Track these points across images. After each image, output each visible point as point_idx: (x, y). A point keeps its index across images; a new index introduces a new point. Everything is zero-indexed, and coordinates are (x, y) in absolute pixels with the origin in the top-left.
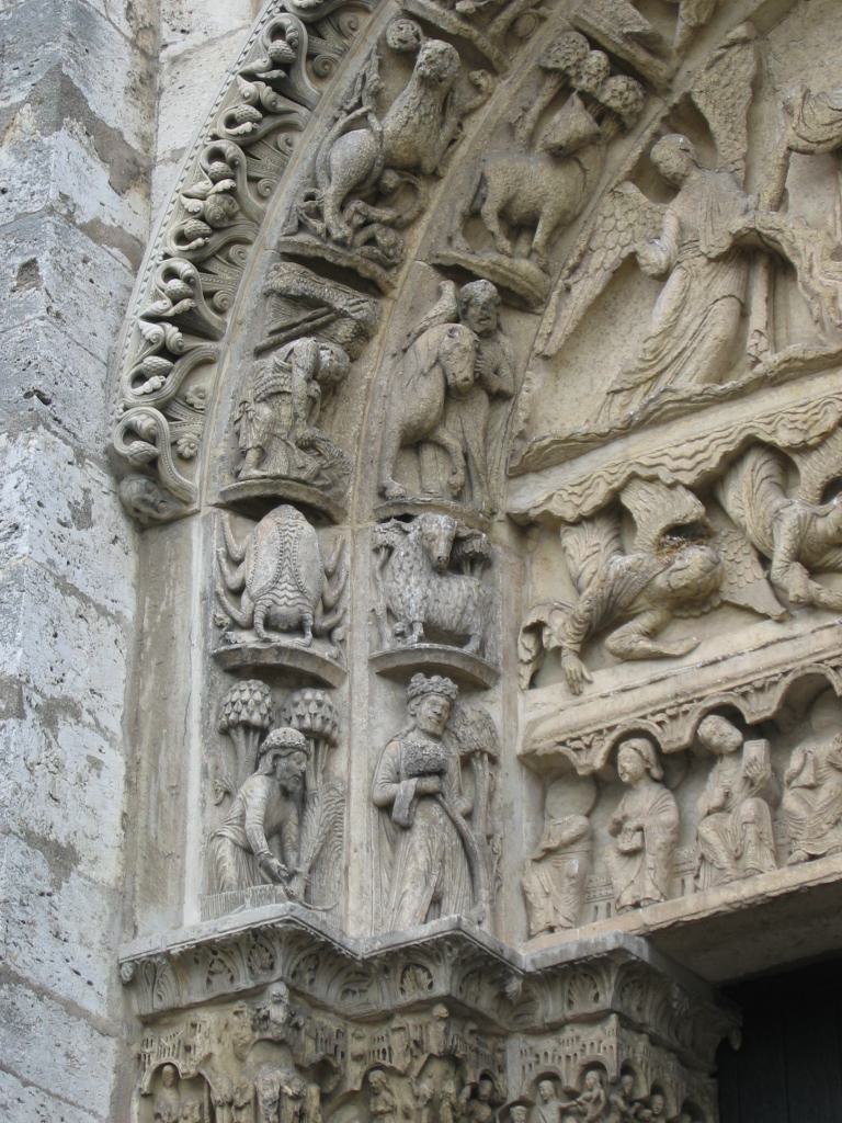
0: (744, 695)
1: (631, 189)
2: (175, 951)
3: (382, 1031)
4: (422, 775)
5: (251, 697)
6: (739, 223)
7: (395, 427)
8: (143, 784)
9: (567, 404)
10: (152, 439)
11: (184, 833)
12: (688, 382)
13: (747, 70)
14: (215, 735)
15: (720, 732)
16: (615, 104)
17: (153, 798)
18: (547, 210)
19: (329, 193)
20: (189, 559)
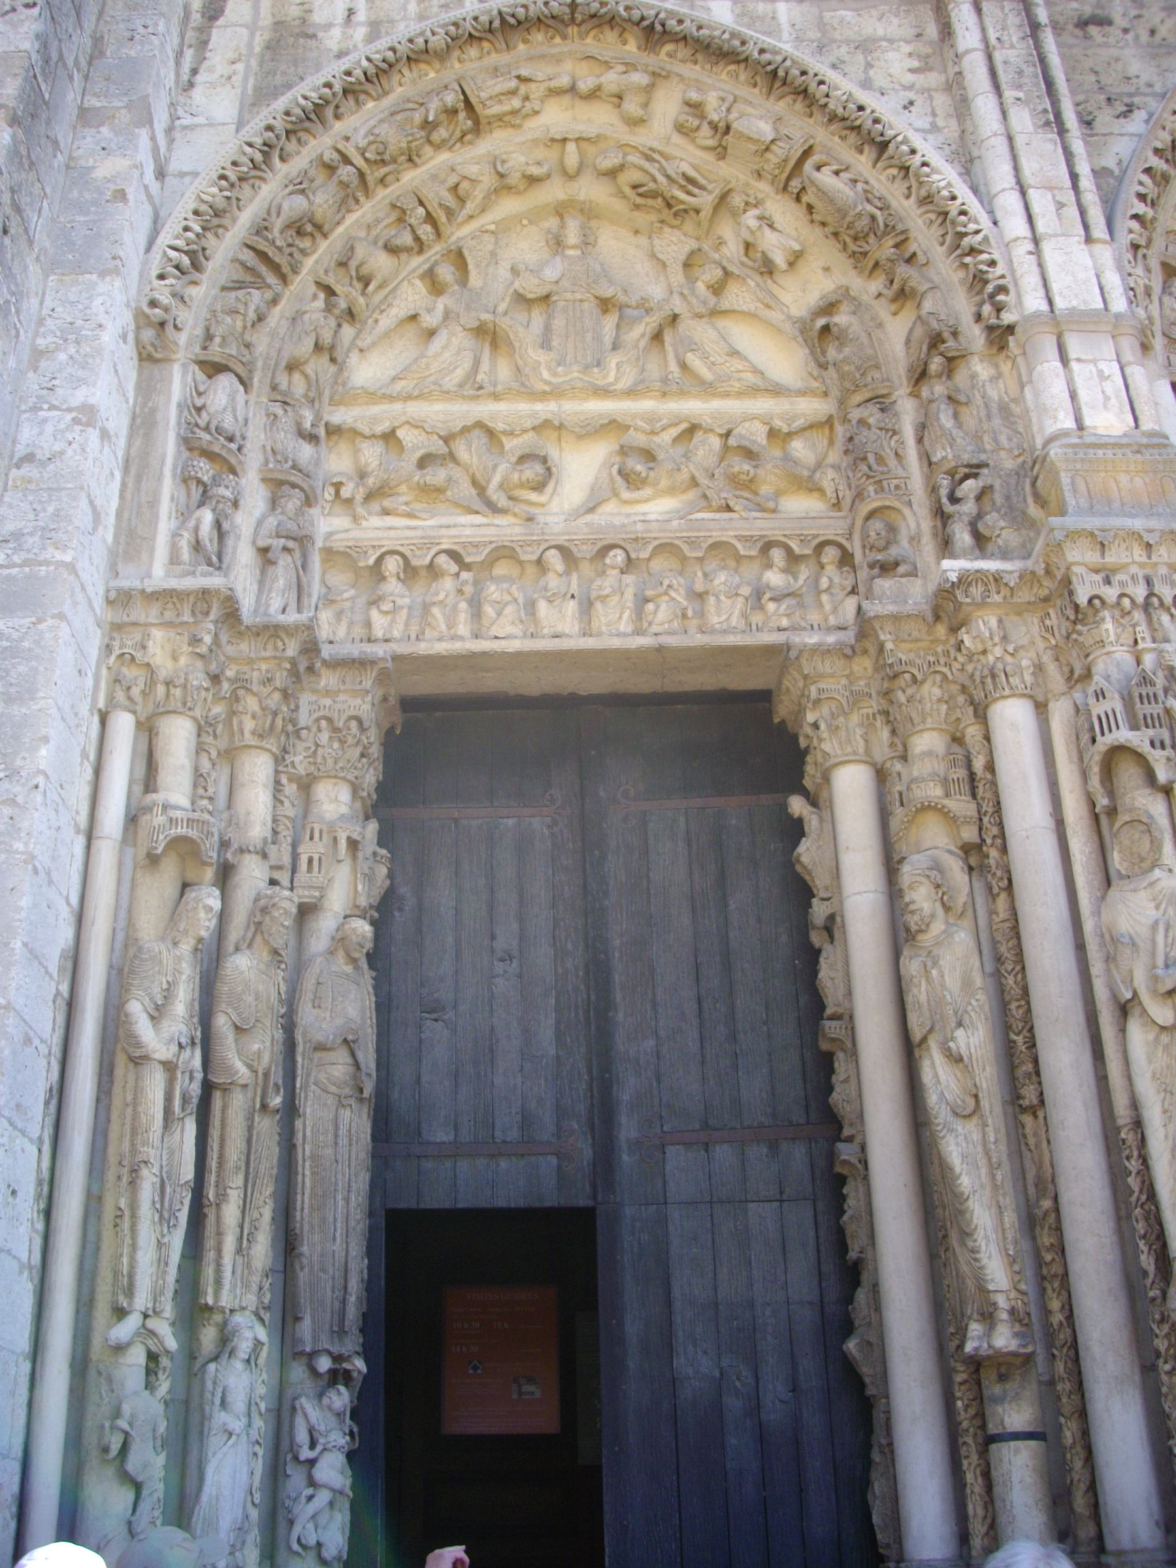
1: (418, 283)
2: (149, 590)
4: (287, 537)
6: (486, 317)
8: (128, 496)
14: (178, 480)
19: (278, 224)
20: (171, 383)
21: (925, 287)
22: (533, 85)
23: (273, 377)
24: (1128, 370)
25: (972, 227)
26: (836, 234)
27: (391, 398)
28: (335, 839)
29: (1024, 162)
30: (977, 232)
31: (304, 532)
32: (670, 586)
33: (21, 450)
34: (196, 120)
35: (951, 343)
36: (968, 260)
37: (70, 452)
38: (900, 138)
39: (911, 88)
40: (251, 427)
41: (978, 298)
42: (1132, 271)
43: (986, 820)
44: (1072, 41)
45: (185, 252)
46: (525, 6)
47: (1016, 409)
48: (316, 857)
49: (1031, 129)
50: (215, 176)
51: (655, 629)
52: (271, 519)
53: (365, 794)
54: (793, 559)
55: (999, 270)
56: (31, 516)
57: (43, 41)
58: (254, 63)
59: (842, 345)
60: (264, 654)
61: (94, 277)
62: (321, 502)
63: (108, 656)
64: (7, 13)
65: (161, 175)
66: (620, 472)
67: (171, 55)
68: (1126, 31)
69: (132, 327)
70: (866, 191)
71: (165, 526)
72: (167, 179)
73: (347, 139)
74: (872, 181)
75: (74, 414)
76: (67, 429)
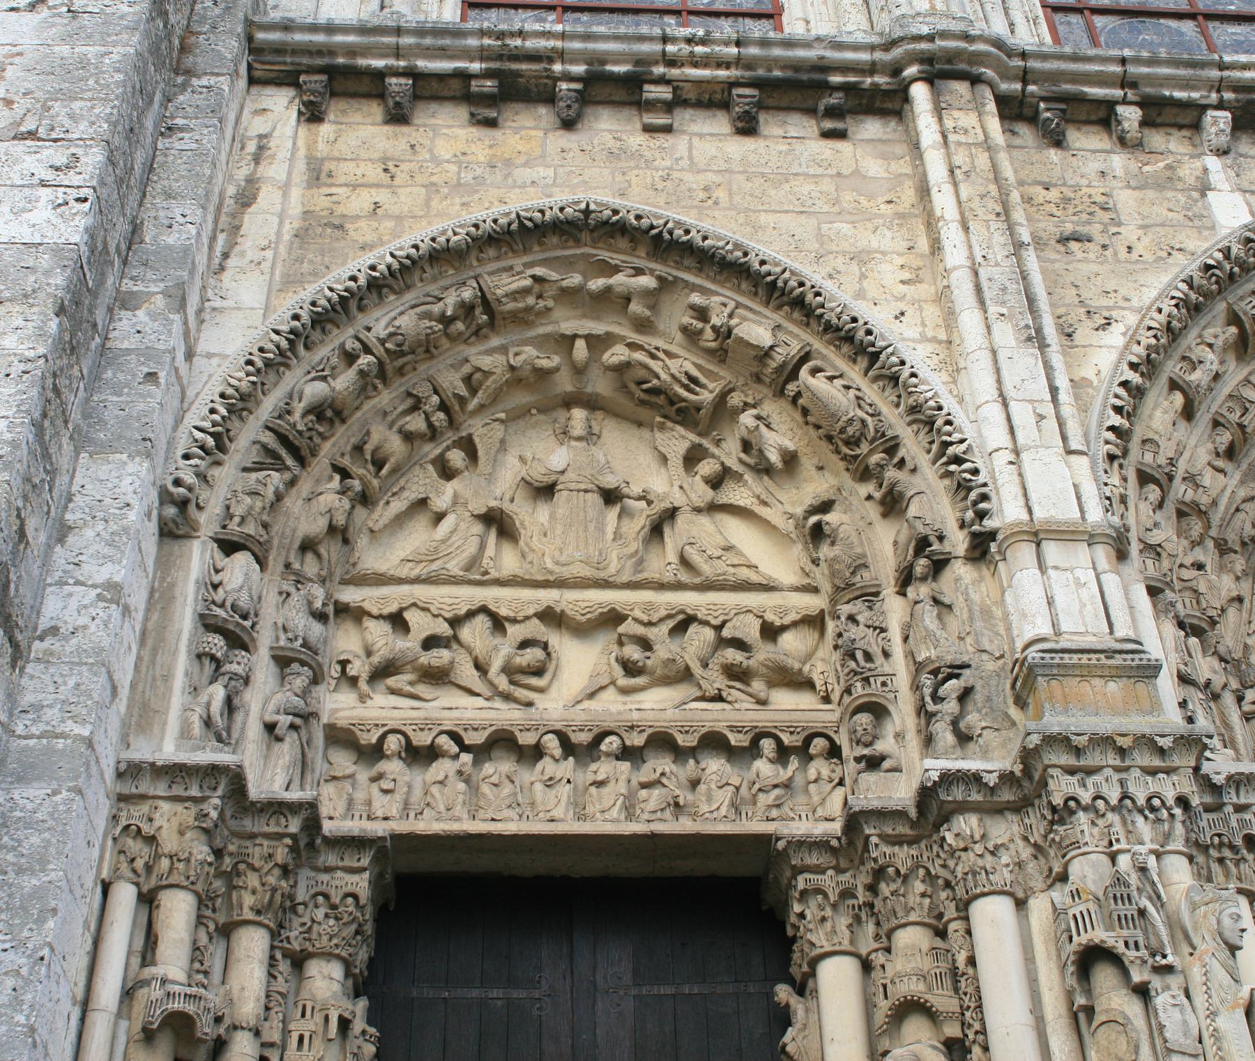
0: (466, 729)
1: (430, 467)
2: (160, 763)
3: (248, 843)
4: (295, 715)
5: (217, 644)
6: (493, 504)
7: (300, 535)
8: (144, 669)
9: (373, 559)
10: (190, 489)
11: (169, 702)
12: (454, 567)
13: (500, 434)
14: (193, 656)
15: (445, 742)
16: (437, 424)
17: (150, 678)
18: (392, 460)
19: (299, 408)
20: (190, 560)
21: (912, 493)
22: (547, 286)
23: (287, 557)
24: (1103, 577)
25: (956, 436)
26: (829, 438)
27: (401, 581)
28: (327, 1018)
29: (1005, 373)
30: (962, 441)
31: (310, 709)
32: (663, 774)
33: (44, 623)
34: (225, 304)
35: (936, 546)
36: (953, 468)
37: (93, 628)
38: (890, 350)
39: (902, 298)
40: (264, 604)
41: (962, 505)
42: (1109, 481)
43: (968, 1014)
44: (1054, 256)
45: (211, 434)
46: (542, 212)
47: (998, 613)
48: (307, 1035)
49: (1014, 343)
50: (242, 361)
51: (646, 816)
52: (279, 695)
53: (357, 971)
54: (783, 753)
55: (981, 479)
56: (52, 689)
57: (91, 233)
58: (282, 249)
59: (833, 543)
60: (266, 829)
61: (124, 457)
62: (328, 679)
63: (114, 827)
64: (60, 205)
65: (190, 355)
66: (617, 660)
67: (205, 240)
68: (1104, 247)
69: (156, 504)
70: (858, 398)
71: (177, 699)
72: (195, 359)
73: (369, 329)
74: (864, 387)
75: (99, 591)
76: (91, 605)
